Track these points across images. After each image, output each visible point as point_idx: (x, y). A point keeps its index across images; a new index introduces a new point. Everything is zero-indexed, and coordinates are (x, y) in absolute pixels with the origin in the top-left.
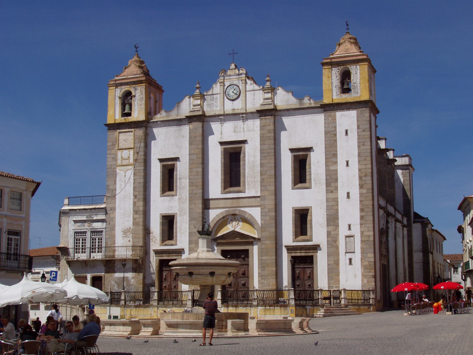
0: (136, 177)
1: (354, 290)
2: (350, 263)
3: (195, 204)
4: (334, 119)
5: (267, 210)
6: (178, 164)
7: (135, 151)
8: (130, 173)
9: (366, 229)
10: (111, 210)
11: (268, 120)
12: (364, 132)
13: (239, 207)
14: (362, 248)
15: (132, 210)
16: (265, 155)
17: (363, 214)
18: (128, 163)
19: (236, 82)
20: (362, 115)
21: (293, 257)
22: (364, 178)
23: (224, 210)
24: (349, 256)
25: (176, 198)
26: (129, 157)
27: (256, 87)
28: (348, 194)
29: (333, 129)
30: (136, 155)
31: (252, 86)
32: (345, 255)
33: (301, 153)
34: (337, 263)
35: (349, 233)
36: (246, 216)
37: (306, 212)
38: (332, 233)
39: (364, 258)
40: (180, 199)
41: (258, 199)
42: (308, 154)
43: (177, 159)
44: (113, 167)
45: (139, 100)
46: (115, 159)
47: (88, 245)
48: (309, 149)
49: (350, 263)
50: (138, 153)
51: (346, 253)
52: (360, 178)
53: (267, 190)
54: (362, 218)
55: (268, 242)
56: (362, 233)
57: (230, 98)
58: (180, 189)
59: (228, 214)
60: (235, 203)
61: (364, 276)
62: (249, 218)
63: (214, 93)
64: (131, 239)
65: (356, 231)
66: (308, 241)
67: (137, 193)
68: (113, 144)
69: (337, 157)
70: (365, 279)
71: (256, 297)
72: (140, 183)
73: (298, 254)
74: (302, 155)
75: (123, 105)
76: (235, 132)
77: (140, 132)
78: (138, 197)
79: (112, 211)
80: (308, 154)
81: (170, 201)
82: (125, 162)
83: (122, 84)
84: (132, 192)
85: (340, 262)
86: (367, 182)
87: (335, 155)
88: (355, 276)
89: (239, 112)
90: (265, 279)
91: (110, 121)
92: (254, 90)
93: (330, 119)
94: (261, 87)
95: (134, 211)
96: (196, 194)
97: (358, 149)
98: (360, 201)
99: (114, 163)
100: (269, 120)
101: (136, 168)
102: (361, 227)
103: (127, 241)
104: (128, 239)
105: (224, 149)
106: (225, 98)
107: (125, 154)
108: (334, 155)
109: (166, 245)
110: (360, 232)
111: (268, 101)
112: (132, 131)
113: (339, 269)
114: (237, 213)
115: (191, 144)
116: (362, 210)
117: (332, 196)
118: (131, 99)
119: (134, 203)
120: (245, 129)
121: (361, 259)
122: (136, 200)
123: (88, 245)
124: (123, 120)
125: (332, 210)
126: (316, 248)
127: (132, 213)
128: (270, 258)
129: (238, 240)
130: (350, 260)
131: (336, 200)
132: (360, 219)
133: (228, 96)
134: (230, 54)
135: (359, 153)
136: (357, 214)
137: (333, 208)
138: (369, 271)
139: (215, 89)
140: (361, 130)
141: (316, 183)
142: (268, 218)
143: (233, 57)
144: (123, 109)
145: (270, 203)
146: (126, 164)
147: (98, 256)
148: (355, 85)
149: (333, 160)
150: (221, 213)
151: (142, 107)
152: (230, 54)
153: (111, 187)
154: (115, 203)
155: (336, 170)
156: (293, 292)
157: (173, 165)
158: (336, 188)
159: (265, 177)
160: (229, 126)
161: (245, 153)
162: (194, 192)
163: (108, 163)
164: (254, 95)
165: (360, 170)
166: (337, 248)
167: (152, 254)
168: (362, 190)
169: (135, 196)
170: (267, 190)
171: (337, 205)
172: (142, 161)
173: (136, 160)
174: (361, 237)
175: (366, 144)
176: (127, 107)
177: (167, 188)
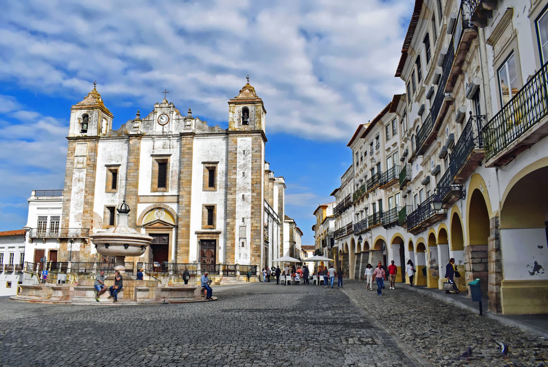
0: (88, 178)
1: (245, 265)
2: (243, 246)
3: (131, 199)
5: (184, 205)
7: (88, 158)
8: (83, 174)
9: (255, 221)
10: (67, 200)
11: (188, 141)
12: (256, 153)
13: (163, 202)
14: (251, 235)
15: (83, 202)
16: (184, 165)
17: (253, 211)
18: (82, 167)
19: (166, 112)
20: (255, 141)
22: (255, 185)
23: (152, 204)
24: (242, 240)
25: (117, 194)
26: (83, 163)
27: (181, 117)
28: (243, 195)
29: (235, 149)
30: (88, 161)
31: (178, 116)
32: (240, 240)
33: (211, 165)
34: (233, 245)
35: (241, 224)
36: (168, 209)
37: (212, 208)
38: (231, 223)
39: (253, 242)
40: (120, 195)
42: (215, 167)
43: (119, 165)
44: (70, 169)
45: (94, 121)
46: (72, 163)
47: (48, 226)
48: (217, 163)
49: (243, 246)
50: (90, 160)
51: (240, 238)
52: (252, 185)
53: (185, 191)
54: (252, 213)
55: (184, 229)
56: (252, 224)
57: (161, 124)
58: (121, 187)
59: (155, 207)
60: (161, 199)
61: (252, 255)
62: (170, 211)
63: (150, 119)
64: (81, 223)
65: (248, 222)
66: (213, 229)
67: (87, 189)
68: (71, 152)
69: (236, 169)
70: (253, 257)
71: (172, 269)
72: (90, 182)
73: (205, 238)
74: (212, 167)
75: (82, 124)
76: (163, 147)
78: (88, 192)
79: (67, 202)
80: (215, 167)
81: (112, 196)
82: (80, 166)
83: (81, 109)
84: (84, 187)
85: (236, 244)
86: (256, 188)
87: (235, 168)
88: (246, 256)
89: (167, 134)
90: (180, 256)
91: (71, 135)
92: (179, 119)
93: (233, 142)
95: (84, 202)
96: (131, 191)
97: (252, 164)
98: (252, 201)
99: (72, 166)
101: (88, 171)
102: (251, 220)
103: (78, 224)
104: (80, 223)
106: (157, 123)
108: (234, 167)
110: (250, 224)
111: (189, 127)
112: (87, 144)
113: (234, 250)
114: (162, 207)
116: (252, 208)
118: (88, 120)
119: (85, 197)
120: (171, 147)
121: (251, 243)
122: (87, 194)
123: (48, 226)
124: (80, 135)
125: (231, 207)
126: (218, 233)
127: (83, 203)
128: (184, 240)
129: (162, 226)
130: (243, 243)
131: (234, 200)
132: (251, 214)
133: (159, 122)
134: (163, 93)
135: (252, 167)
136: (249, 209)
137: (232, 205)
138: (256, 251)
139: (150, 117)
140: (255, 151)
141: (220, 188)
142: (184, 211)
143: (165, 94)
146: (81, 167)
147: (54, 235)
148: (252, 119)
149: (234, 171)
151: (96, 126)
152: (163, 93)
153: (68, 184)
154: (70, 196)
155: (236, 179)
156: (200, 265)
157: (116, 170)
158: (235, 191)
159: (183, 181)
160: (159, 143)
161: (170, 164)
162: (130, 190)
163: (67, 166)
164: (179, 122)
165: (252, 179)
166: (234, 234)
168: (253, 193)
169: (86, 192)
170: (185, 191)
171: (235, 204)
172: (92, 165)
173: (88, 165)
174: (251, 227)
175: (257, 161)
176: (85, 125)
177: (110, 187)
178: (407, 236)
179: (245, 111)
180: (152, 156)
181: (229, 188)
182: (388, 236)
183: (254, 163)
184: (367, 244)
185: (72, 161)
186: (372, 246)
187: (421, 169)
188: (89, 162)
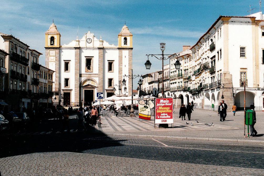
4: (122, 52)
6: (70, 62)
17: (129, 81)
21: (107, 93)
23: (86, 77)
26: (53, 59)
33: (111, 62)
41: (97, 75)
43: (70, 61)
52: (129, 70)
60: (89, 76)
68: (47, 54)
77: (57, 51)
87: (122, 63)
94: (99, 40)
99: (48, 60)
100: (102, 51)
105: (86, 59)
107: (52, 58)
109: (66, 88)
114: (90, 79)
115: (75, 56)
117: (120, 75)
124: (51, 46)
142: (101, 81)
144: (51, 43)
145: (101, 76)
150: (85, 79)
155: (122, 68)
158: (122, 73)
165: (129, 68)
167: (62, 91)
173: (56, 60)
176: (52, 42)
178: (190, 95)
179: (125, 39)
180: (85, 57)
181: (120, 71)
182: (184, 94)
183: (130, 61)
184: (175, 96)
185: (48, 58)
186: (177, 96)
187: (195, 79)
188: (56, 59)
